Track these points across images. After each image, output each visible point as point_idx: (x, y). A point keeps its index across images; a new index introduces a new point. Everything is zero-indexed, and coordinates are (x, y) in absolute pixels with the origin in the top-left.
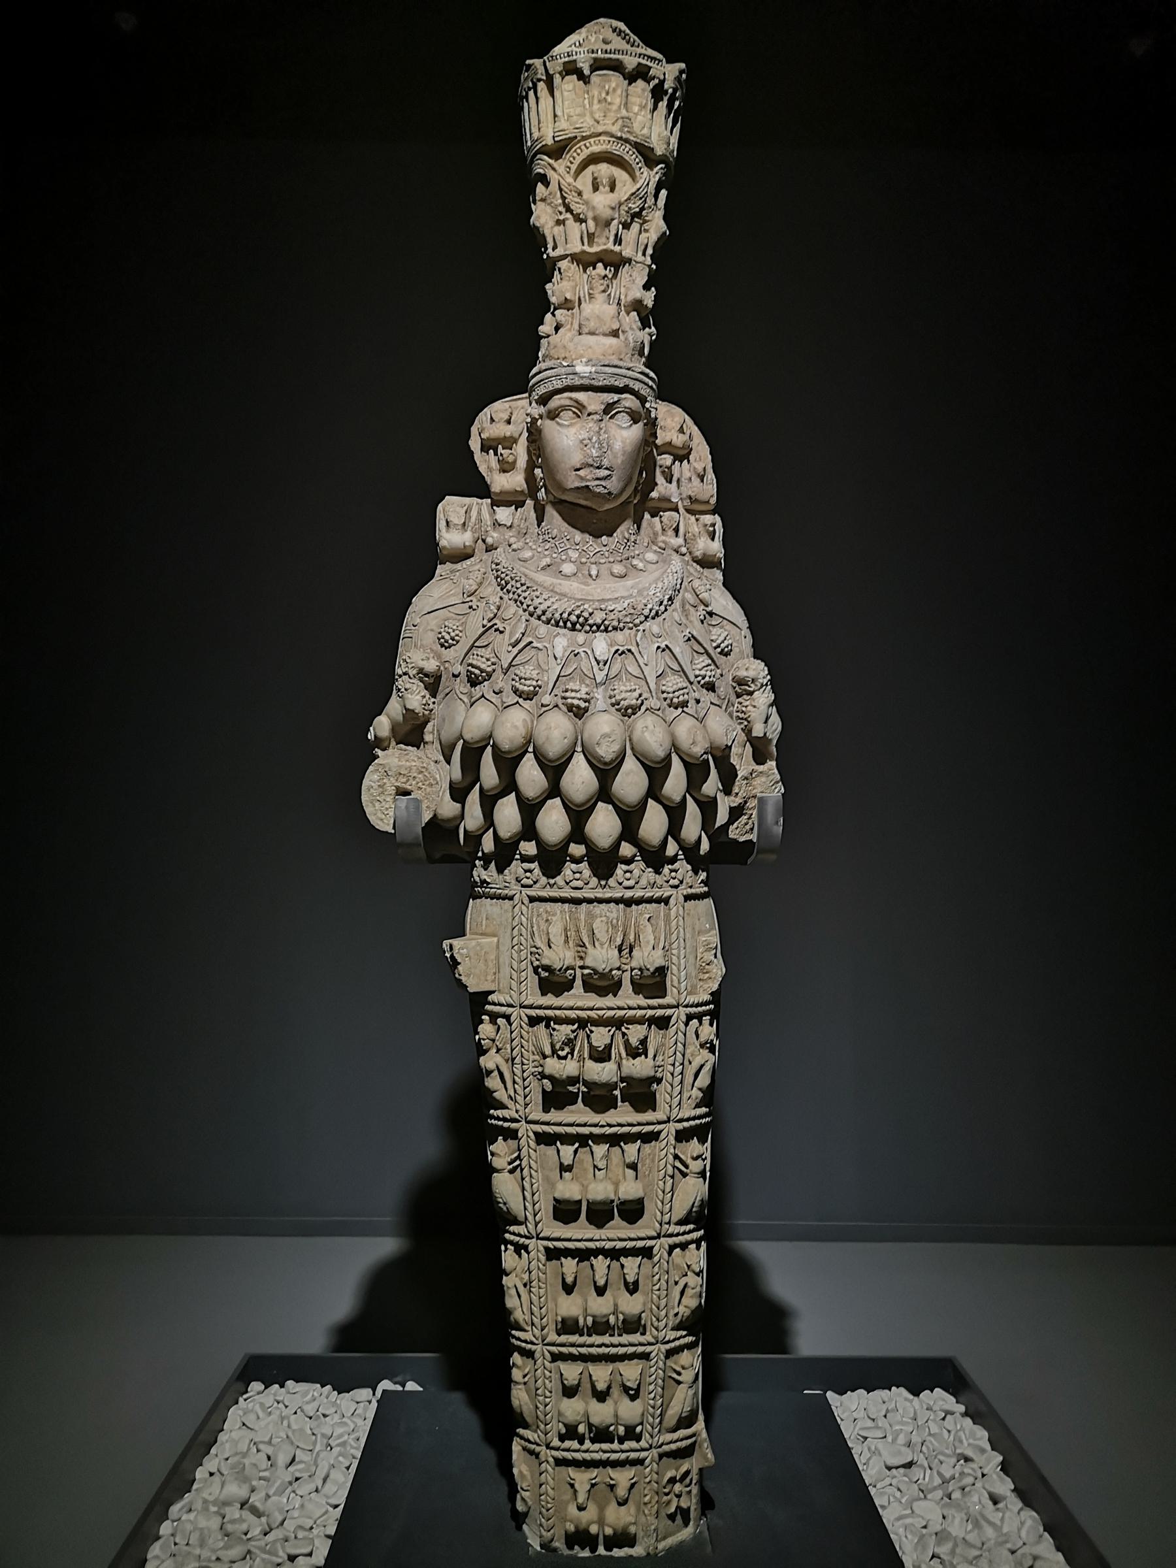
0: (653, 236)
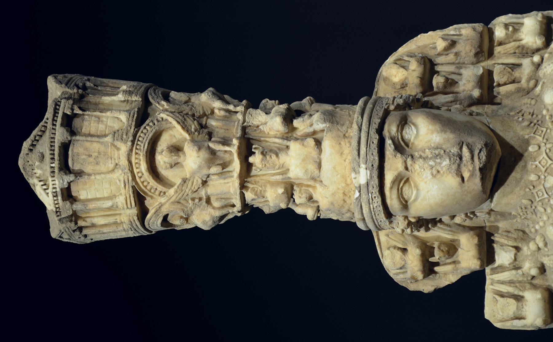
0: (217, 104)
